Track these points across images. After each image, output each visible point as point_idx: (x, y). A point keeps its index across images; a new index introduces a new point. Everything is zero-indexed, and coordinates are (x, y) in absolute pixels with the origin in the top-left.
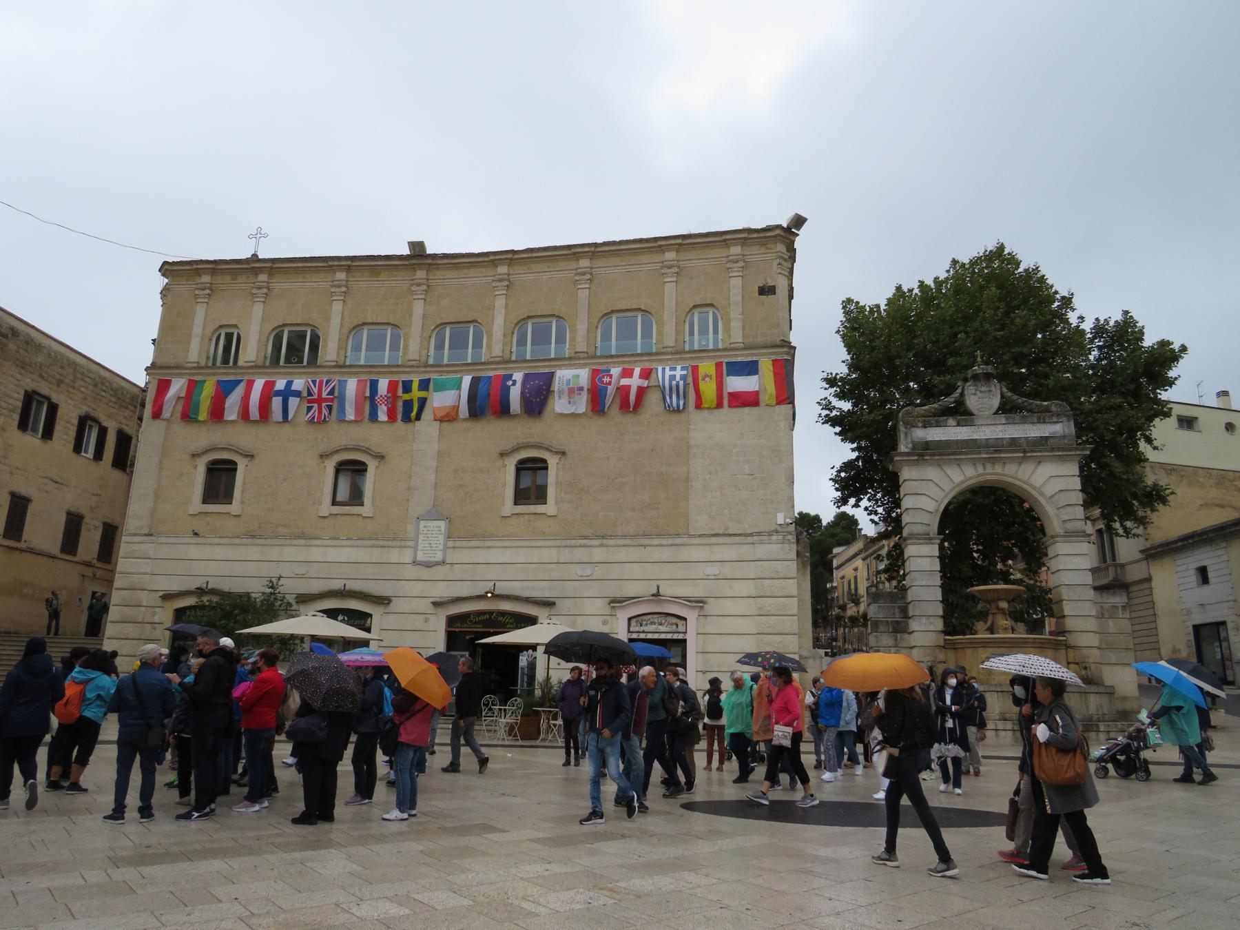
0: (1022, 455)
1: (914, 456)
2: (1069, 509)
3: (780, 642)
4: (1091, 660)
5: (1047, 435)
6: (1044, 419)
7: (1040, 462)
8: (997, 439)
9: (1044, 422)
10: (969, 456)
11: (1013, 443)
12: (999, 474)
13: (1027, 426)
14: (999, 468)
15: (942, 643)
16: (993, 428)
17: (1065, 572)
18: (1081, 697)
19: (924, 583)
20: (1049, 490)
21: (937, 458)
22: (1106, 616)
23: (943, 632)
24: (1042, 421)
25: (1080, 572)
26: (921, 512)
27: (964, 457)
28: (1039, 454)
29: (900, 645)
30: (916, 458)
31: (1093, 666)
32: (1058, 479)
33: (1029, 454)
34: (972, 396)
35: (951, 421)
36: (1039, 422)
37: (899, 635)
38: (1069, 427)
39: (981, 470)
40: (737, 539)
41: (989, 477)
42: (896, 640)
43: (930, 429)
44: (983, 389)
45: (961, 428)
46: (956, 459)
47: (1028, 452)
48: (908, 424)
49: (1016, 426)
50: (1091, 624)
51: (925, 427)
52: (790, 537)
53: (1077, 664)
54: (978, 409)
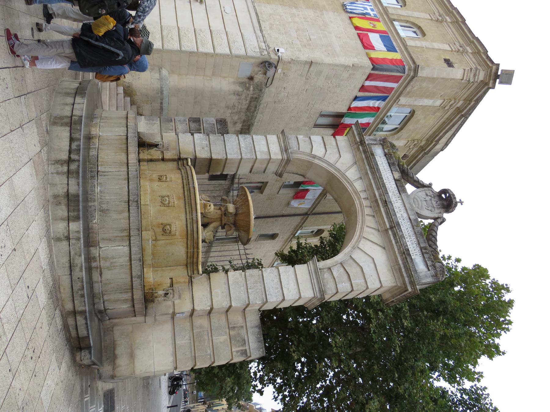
0: (388, 226)
2: (346, 276)
3: (173, 39)
4: (176, 302)
7: (384, 248)
9: (423, 254)
10: (372, 181)
11: (395, 226)
13: (413, 238)
14: (368, 211)
15: (183, 156)
16: (403, 209)
17: (277, 274)
18: (123, 230)
19: (242, 145)
20: (358, 256)
21: (363, 156)
22: (232, 333)
23: (196, 158)
24: (424, 251)
27: (371, 177)
28: (394, 242)
30: (358, 140)
31: (170, 303)
32: (373, 266)
33: (390, 232)
34: (424, 194)
35: (397, 175)
36: (421, 249)
38: (426, 276)
39: (363, 195)
40: (256, 25)
41: (357, 202)
43: (385, 159)
44: (434, 203)
45: (394, 183)
46: (367, 173)
47: (393, 231)
48: (384, 142)
49: (411, 229)
50: (221, 302)
51: (385, 155)
52: (265, 53)
53: (172, 285)
54: (415, 198)
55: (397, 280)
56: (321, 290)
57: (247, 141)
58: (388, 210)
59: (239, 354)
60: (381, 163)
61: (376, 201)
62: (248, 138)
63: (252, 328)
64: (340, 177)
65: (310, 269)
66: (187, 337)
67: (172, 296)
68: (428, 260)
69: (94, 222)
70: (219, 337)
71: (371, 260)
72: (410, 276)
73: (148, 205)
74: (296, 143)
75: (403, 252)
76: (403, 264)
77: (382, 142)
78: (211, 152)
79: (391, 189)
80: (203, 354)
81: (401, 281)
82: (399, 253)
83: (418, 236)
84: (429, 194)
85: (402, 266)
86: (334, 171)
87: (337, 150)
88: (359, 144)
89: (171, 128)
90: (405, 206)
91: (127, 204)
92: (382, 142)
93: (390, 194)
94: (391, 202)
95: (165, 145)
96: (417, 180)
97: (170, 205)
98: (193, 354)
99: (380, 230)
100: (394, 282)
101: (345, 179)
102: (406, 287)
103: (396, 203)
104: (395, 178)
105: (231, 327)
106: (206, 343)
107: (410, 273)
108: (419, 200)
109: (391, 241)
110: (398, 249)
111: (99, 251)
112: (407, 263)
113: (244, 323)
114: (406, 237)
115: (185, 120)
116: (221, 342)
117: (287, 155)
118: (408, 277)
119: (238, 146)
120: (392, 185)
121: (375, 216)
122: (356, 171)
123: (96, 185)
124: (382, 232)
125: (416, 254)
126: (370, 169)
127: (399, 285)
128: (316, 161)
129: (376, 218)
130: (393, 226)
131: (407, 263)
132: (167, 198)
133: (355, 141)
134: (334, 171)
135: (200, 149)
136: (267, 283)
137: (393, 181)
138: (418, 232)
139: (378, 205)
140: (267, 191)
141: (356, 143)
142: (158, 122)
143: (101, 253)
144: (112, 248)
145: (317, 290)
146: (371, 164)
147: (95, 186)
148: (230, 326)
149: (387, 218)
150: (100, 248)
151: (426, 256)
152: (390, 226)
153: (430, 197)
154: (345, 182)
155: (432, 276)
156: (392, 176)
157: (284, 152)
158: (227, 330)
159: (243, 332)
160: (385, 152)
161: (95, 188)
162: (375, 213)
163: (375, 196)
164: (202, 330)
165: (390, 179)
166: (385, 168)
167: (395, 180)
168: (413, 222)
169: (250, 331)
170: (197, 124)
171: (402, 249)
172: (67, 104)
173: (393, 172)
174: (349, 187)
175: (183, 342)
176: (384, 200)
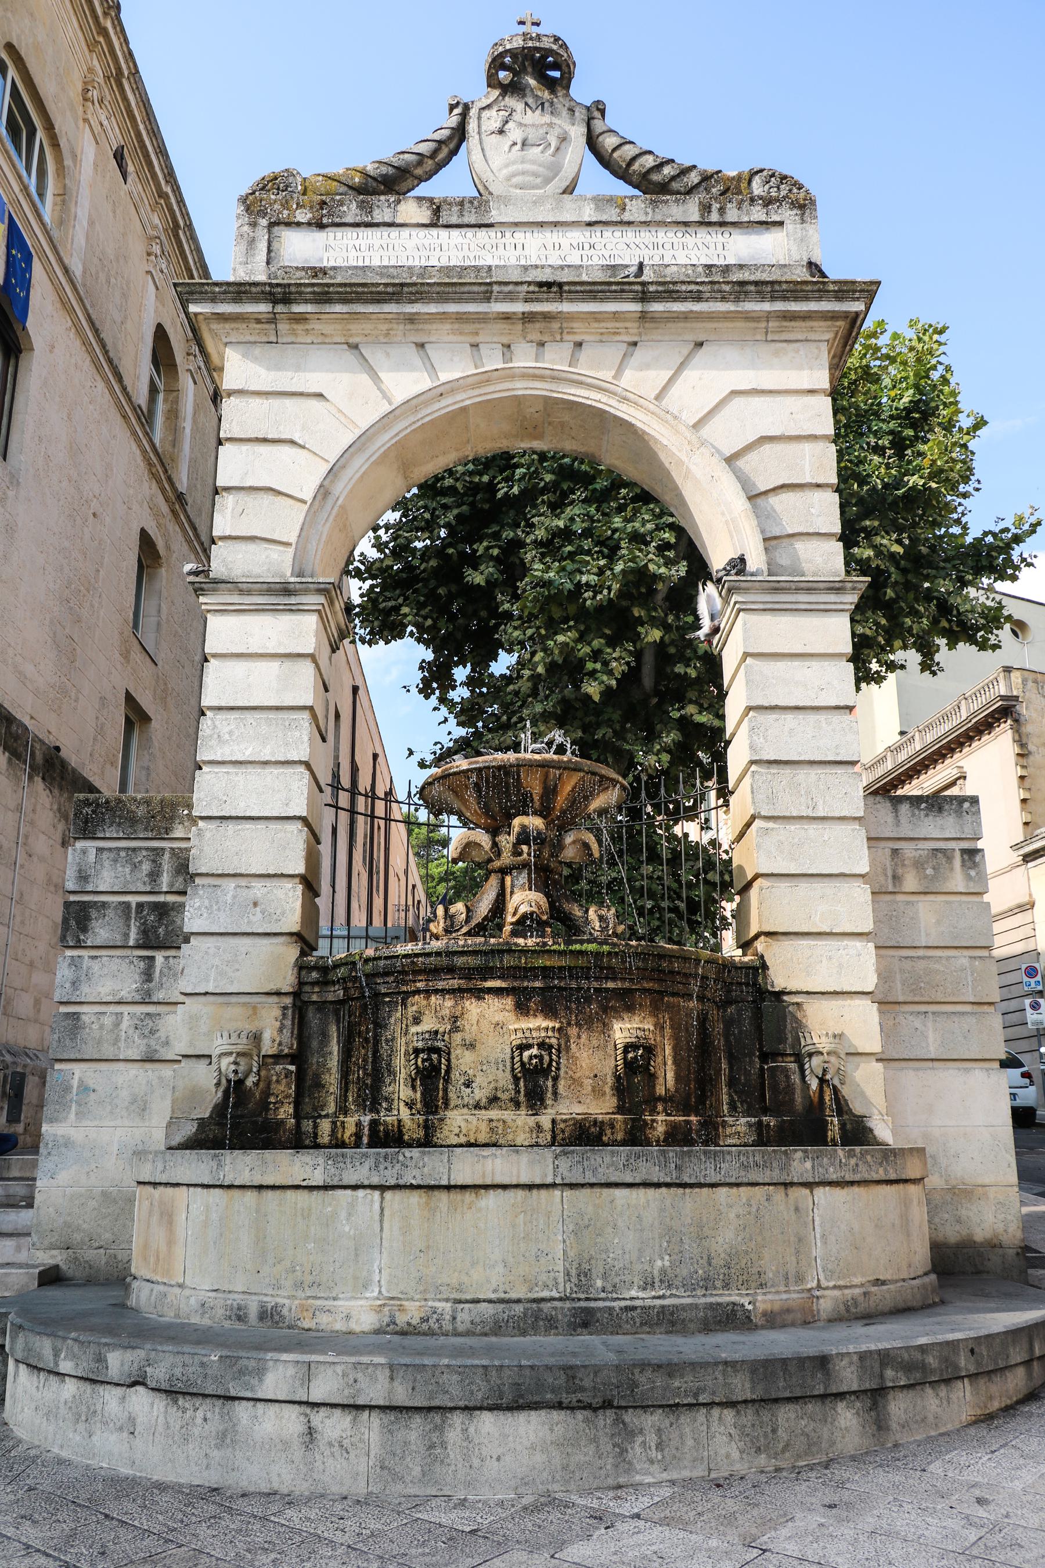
0: (635, 307)
1: (256, 300)
5: (731, 261)
6: (722, 210)
8: (562, 267)
9: (722, 224)
10: (452, 308)
12: (555, 377)
14: (556, 358)
16: (550, 237)
21: (338, 308)
25: (822, 717)
26: (267, 499)
27: (432, 308)
28: (697, 307)
29: (160, 996)
30: (263, 308)
32: (757, 401)
33: (657, 307)
37: (159, 957)
39: (493, 361)
41: (521, 388)
42: (148, 975)
45: (444, 233)
46: (411, 319)
51: (321, 226)
55: (812, 336)
56: (837, 585)
57: (230, 733)
58: (578, 288)
59: (973, 873)
60: (353, 253)
61: (528, 318)
62: (215, 727)
63: (898, 823)
64: (412, 419)
65: (761, 606)
66: (917, 1023)
67: (833, 1059)
68: (748, 213)
69: (750, 1307)
70: (922, 925)
71: (738, 401)
72: (819, 291)
73: (554, 1121)
74: (251, 547)
75: (737, 288)
76: (773, 299)
77: (264, 222)
78: (275, 876)
79: (466, 252)
80: (970, 979)
81: (822, 324)
82: (737, 300)
83: (658, 218)
84: (496, 125)
85: (780, 306)
86: (387, 436)
87: (288, 402)
88: (279, 308)
89: (108, 1021)
90: (541, 225)
91: (688, 1190)
92: (264, 222)
93: (489, 261)
94: (526, 268)
95: (239, 1048)
96: (432, 146)
97: (554, 1041)
98: (968, 1008)
99: (635, 339)
100: (818, 348)
101: (426, 403)
102: (845, 315)
103: (527, 252)
104: (426, 221)
105: (894, 885)
106: (937, 966)
107: (809, 288)
108: (520, 167)
109: (686, 317)
110: (723, 299)
111: (827, 1288)
112: (777, 287)
113: (883, 844)
114: (657, 260)
115: (74, 962)
116: (938, 922)
117: (306, 592)
118: (820, 299)
119: (250, 769)
120: (452, 243)
121: (578, 338)
122: (388, 354)
123: (623, 1304)
124: (640, 334)
125: (720, 247)
126: (398, 302)
127: (829, 336)
128: (341, 488)
129: (586, 337)
130: (638, 288)
131: (777, 287)
132: (526, 1054)
133: (258, 321)
134: (387, 436)
135: (259, 916)
136: (800, 754)
137: (434, 232)
138: (647, 214)
139: (547, 317)
140: (145, 701)
141: (273, 319)
142: (77, 1069)
143: (831, 1284)
144: (819, 1244)
145: (832, 598)
146: (381, 288)
147: (628, 1309)
148: (891, 889)
149: (602, 300)
150: (819, 1287)
151: (732, 215)
152: (634, 300)
153: (511, 125)
154: (437, 406)
155: (803, 221)
156: (414, 232)
157: (293, 600)
158: (900, 898)
159: (909, 850)
160: (309, 224)
161: (634, 1308)
162: (566, 337)
163: (507, 317)
164: (898, 976)
165: (426, 242)
166: (377, 243)
167: (433, 225)
168: (604, 218)
169: (906, 831)
170: (94, 914)
171: (727, 288)
172: (311, 1431)
173: (398, 221)
174: (459, 397)
175: (931, 1039)
176: (532, 288)
